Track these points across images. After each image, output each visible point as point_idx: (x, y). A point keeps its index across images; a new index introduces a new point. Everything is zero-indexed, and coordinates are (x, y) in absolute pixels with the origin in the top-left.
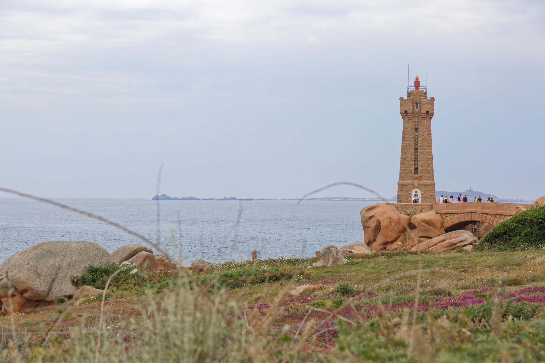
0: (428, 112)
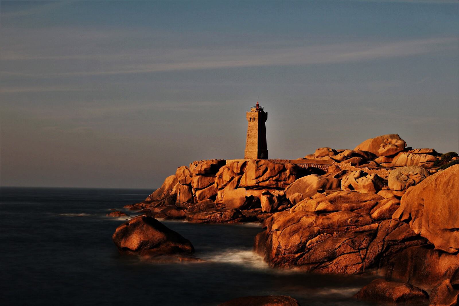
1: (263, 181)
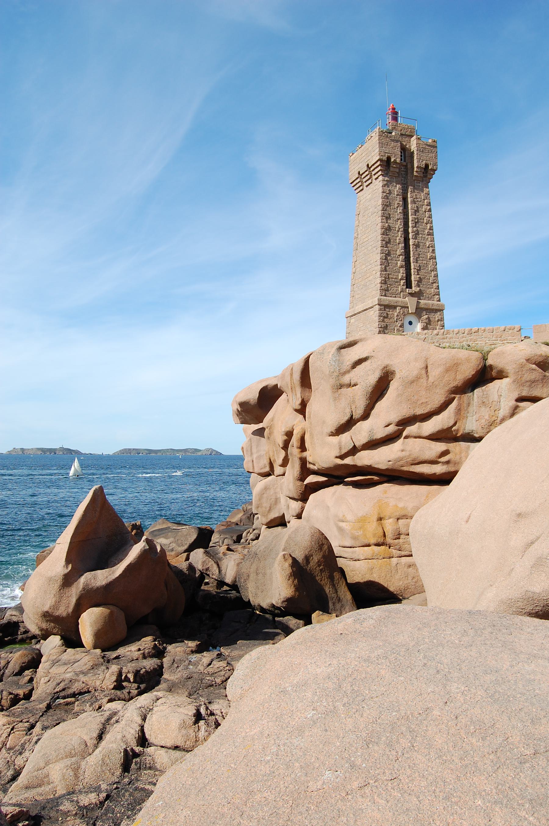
0: (427, 166)
1: (373, 444)
